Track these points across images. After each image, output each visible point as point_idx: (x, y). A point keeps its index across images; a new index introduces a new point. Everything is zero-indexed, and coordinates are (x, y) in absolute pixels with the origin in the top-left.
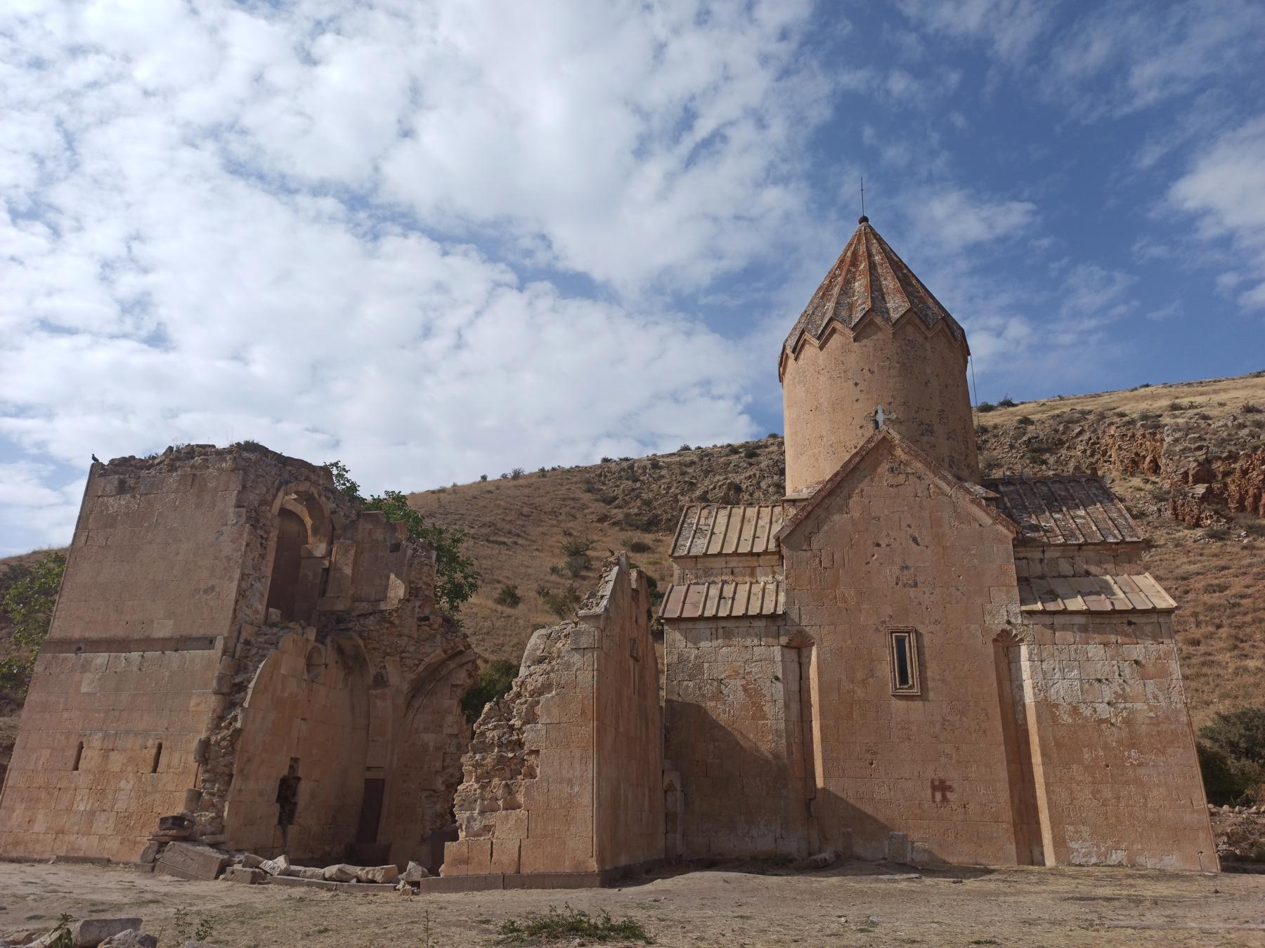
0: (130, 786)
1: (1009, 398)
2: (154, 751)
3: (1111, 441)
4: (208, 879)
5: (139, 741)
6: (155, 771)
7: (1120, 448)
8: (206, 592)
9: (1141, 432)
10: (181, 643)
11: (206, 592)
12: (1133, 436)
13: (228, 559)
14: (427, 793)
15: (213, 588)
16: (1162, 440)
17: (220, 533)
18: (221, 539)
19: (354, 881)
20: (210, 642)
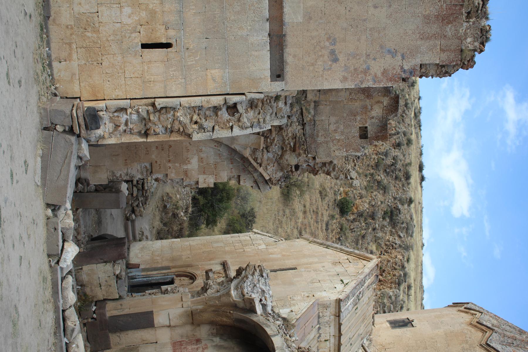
0: (126, 20)
1: (426, 180)
2: (164, 41)
3: (393, 256)
4: (44, 195)
5: (172, 18)
6: (145, 46)
7: (389, 261)
8: (332, 52)
9: (397, 274)
10: (278, 41)
11: (332, 52)
12: (395, 269)
13: (366, 71)
14: (149, 167)
15: (336, 60)
16: (391, 288)
17: (393, 53)
18: (388, 57)
19: (65, 340)
20: (278, 75)
